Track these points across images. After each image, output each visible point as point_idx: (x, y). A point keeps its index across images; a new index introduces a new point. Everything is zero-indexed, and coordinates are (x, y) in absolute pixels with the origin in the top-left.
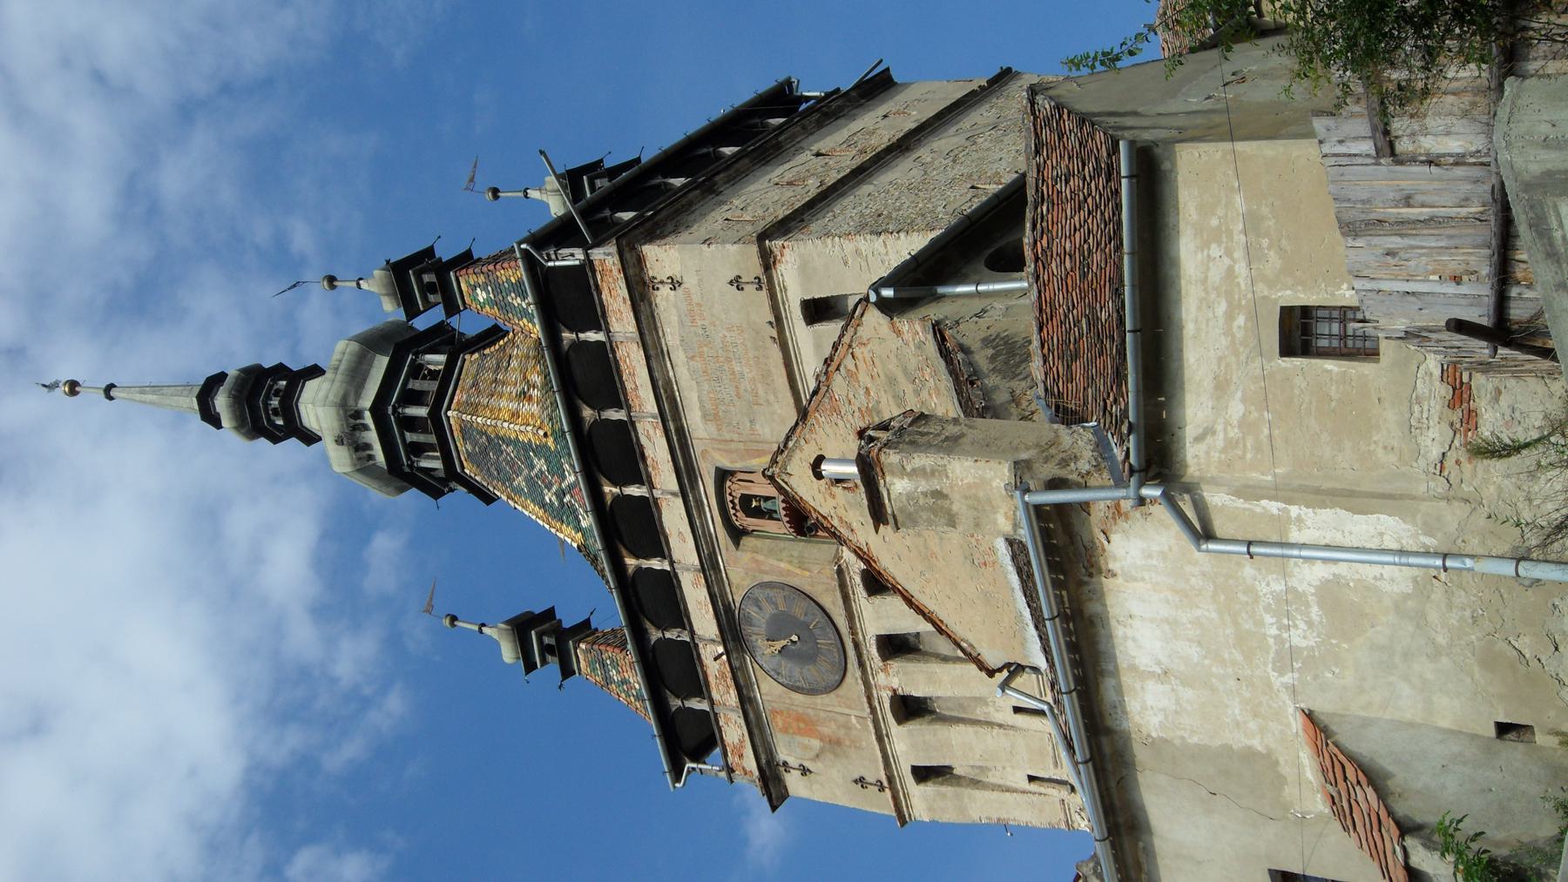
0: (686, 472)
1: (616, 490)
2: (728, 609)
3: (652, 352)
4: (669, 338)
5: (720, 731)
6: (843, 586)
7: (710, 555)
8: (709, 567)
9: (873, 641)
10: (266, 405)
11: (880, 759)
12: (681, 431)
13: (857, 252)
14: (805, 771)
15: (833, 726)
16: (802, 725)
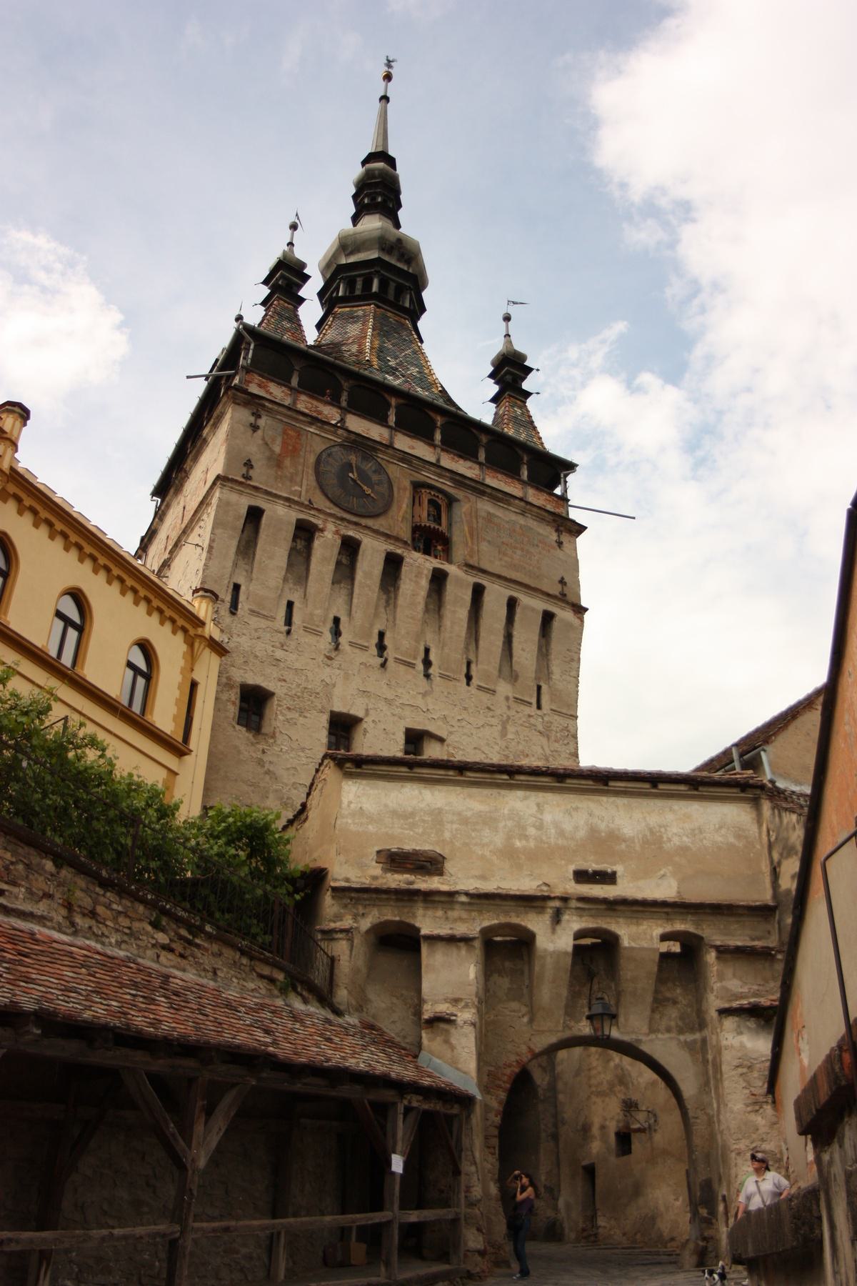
0: (460, 480)
1: (439, 424)
2: (375, 450)
3: (528, 507)
4: (531, 521)
5: (279, 384)
6: (397, 539)
7: (411, 462)
8: (406, 458)
9: (357, 537)
10: (379, 194)
11: (274, 491)
12: (482, 493)
13: (572, 660)
14: (255, 428)
15: (291, 470)
16: (290, 448)
